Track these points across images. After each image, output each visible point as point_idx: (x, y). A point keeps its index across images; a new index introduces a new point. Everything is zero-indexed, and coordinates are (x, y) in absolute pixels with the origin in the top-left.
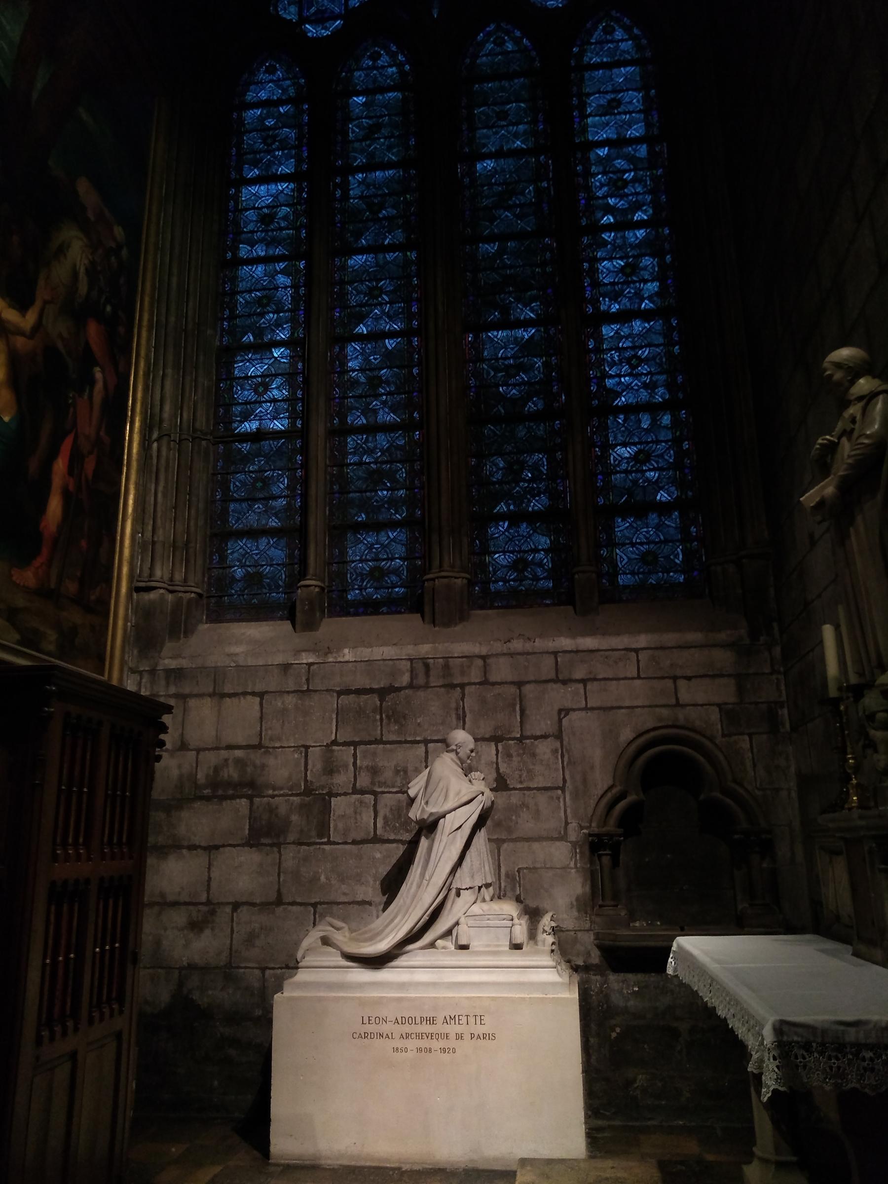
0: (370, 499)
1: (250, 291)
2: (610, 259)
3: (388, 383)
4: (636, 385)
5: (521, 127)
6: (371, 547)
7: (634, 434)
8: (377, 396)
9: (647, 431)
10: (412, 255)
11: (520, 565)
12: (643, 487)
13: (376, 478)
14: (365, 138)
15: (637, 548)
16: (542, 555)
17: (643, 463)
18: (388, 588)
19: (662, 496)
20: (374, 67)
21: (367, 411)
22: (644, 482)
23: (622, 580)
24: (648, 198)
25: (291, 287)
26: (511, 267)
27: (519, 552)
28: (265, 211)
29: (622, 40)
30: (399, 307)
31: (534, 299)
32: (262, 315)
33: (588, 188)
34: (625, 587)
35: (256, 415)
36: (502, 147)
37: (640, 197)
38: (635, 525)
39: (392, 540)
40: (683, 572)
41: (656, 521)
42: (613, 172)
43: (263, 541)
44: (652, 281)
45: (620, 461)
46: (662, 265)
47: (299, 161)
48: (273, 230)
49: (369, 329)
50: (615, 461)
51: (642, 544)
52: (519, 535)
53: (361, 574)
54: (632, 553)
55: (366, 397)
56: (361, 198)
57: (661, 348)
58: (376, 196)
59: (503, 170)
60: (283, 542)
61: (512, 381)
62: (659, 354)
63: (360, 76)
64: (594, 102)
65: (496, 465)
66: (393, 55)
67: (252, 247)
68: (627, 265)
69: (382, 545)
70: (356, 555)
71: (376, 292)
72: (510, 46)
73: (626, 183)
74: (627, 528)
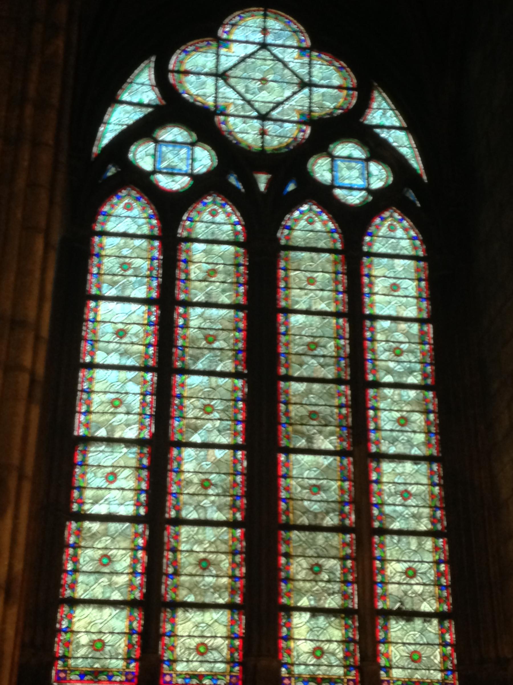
0: (198, 583)
1: (105, 392)
2: (391, 410)
3: (215, 485)
4: (407, 514)
5: (326, 294)
6: (197, 626)
7: (405, 553)
8: (207, 495)
9: (415, 552)
10: (239, 383)
11: (318, 653)
12: (411, 597)
13: (204, 565)
14: (204, 280)
15: (407, 648)
16: (334, 646)
17: (412, 577)
18: (211, 662)
19: (425, 607)
20: (213, 223)
21: (198, 507)
22: (413, 593)
23: (396, 673)
24: (419, 366)
25: (141, 394)
26: (316, 405)
27: (318, 641)
28: (120, 326)
29: (401, 238)
30: (228, 425)
31: (332, 434)
32: (114, 414)
33: (373, 351)
34: (398, 680)
35: (106, 500)
36: (311, 306)
37: (413, 364)
38: (405, 628)
39: (216, 621)
40: (441, 671)
41: (421, 627)
42: (393, 342)
43: (108, 611)
44: (420, 432)
45: (395, 574)
46: (428, 422)
47: (150, 288)
48: (125, 343)
49: (203, 439)
50: (391, 573)
51: (410, 644)
52: (318, 627)
53: (189, 649)
54: (404, 651)
55: (198, 495)
56: (199, 328)
57: (426, 487)
58: (211, 329)
59: (311, 325)
60: (125, 613)
61: (314, 498)
62: (424, 491)
63: (201, 227)
64: (380, 285)
65: (300, 565)
66: (228, 215)
67: (108, 354)
68: (402, 417)
69: (207, 624)
70: (185, 632)
71: (209, 409)
72: (318, 226)
73: (402, 352)
74: (399, 630)
